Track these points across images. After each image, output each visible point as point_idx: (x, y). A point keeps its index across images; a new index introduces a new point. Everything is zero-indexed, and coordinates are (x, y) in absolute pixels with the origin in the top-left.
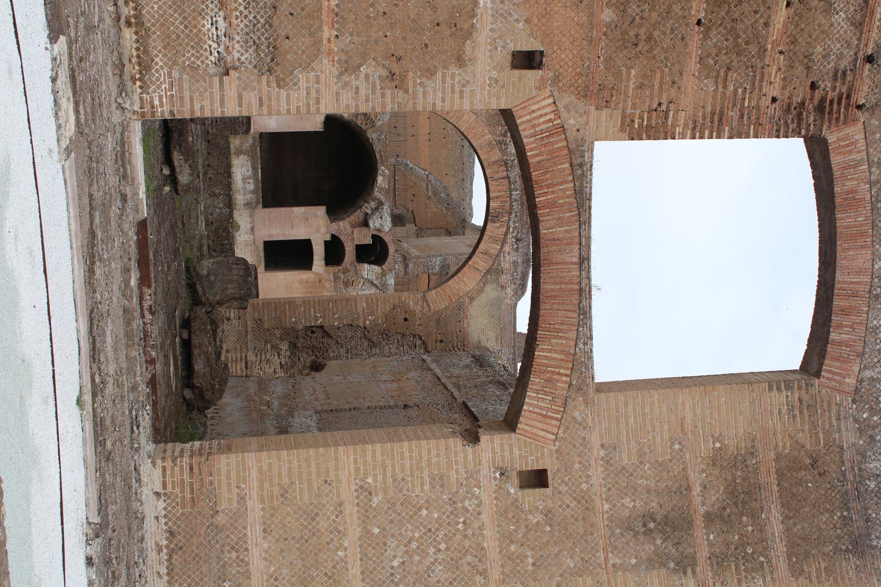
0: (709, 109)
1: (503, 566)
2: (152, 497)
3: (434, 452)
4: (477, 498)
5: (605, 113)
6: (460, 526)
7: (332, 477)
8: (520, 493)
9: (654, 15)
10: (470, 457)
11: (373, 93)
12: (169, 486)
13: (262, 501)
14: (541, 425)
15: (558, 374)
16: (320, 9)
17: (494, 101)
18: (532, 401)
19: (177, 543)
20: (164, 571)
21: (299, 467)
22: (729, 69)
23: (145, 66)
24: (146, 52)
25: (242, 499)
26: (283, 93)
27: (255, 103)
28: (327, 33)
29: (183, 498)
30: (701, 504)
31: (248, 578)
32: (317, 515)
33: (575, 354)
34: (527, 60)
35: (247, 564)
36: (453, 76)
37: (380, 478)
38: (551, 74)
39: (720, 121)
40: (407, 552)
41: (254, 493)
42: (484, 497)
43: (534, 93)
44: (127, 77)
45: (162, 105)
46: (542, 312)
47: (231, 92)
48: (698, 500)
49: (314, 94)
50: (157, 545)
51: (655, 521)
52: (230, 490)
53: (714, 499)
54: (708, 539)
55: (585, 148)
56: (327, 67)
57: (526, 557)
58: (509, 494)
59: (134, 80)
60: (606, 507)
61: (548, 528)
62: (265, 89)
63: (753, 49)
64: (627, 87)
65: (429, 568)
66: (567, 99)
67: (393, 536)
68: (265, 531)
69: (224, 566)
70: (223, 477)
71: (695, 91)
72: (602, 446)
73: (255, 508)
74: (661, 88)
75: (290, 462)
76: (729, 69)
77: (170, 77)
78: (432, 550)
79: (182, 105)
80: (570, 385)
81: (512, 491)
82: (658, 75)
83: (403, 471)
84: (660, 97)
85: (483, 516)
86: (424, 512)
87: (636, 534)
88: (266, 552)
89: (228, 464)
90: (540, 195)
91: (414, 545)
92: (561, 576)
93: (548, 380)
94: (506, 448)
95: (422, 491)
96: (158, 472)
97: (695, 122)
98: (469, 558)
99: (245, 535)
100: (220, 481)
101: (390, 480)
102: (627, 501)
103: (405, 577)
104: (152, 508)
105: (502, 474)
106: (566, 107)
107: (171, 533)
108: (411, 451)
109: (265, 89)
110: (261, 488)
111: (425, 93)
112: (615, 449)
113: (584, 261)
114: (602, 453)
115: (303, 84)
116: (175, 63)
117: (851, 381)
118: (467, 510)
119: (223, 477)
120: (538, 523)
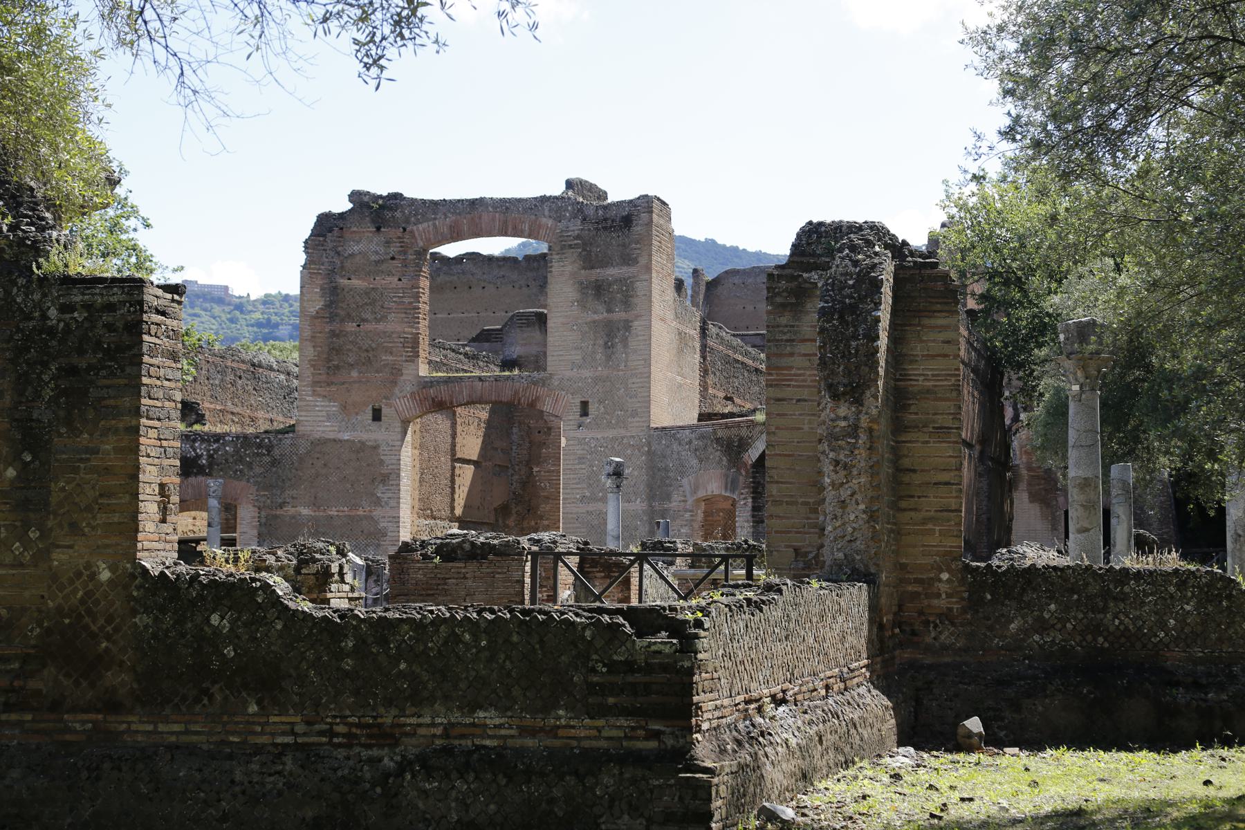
28: (360, 513)
34: (377, 416)
48: (601, 317)
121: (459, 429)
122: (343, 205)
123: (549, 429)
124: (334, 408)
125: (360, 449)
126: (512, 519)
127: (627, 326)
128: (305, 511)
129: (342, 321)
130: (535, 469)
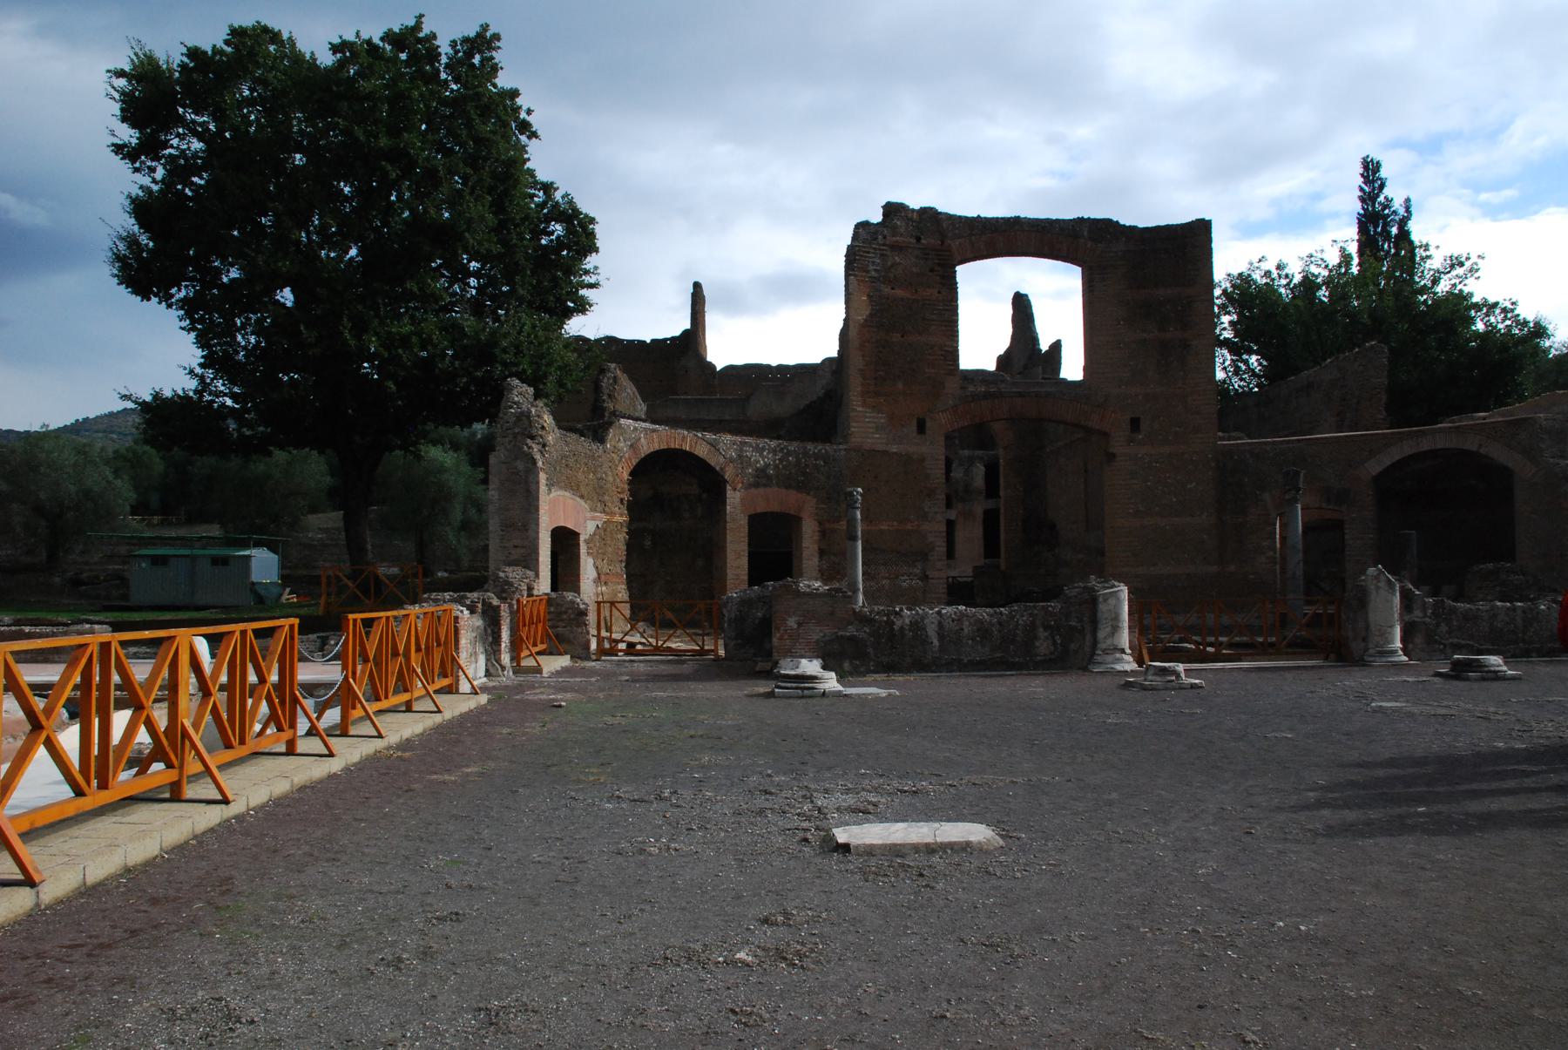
28: (909, 527)
34: (921, 428)
117: (1089, 244)
122: (876, 217)
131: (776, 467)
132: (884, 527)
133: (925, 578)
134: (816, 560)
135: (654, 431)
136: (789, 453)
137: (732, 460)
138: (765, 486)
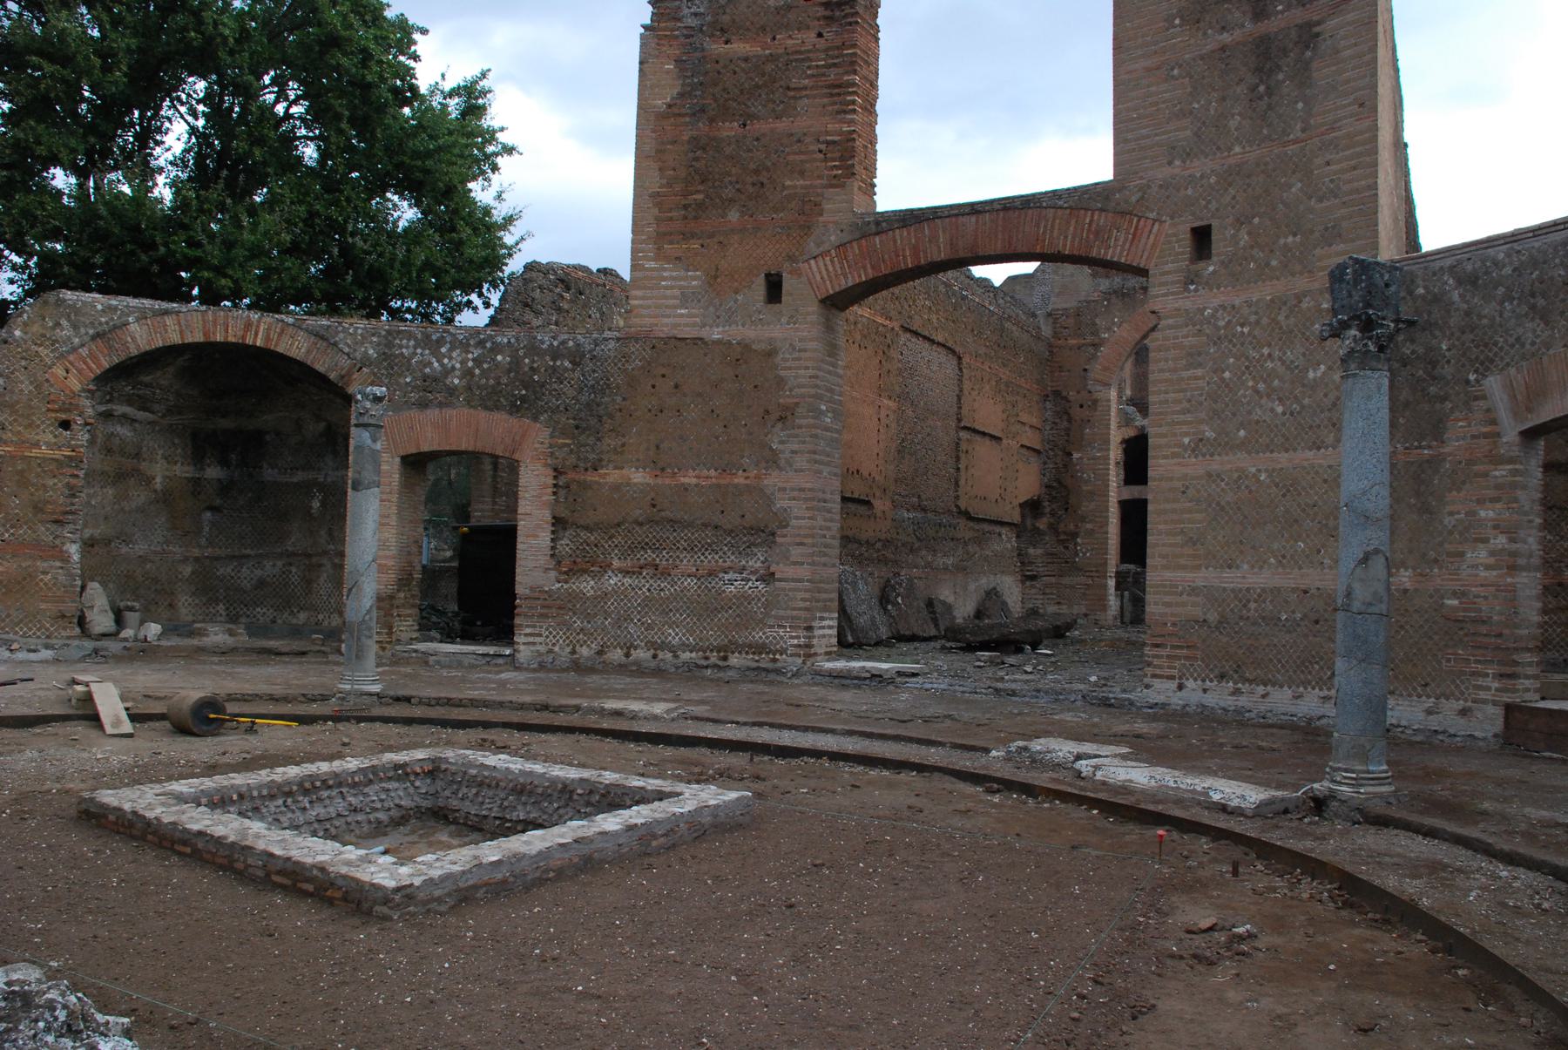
0: (826, 101)
1: (1293, 275)
2: (1183, 694)
3: (1162, 365)
4: (1216, 311)
5: (827, 206)
6: (1246, 330)
7: (1178, 484)
8: (1215, 259)
9: (734, 171)
10: (1170, 321)
11: (797, 436)
12: (1174, 672)
13: (1198, 567)
14: (1143, 241)
15: (1090, 224)
16: (719, 486)
17: (809, 318)
18: (1115, 252)
19: (1230, 670)
20: (1261, 689)
21: (1166, 522)
22: (788, 88)
23: (760, 649)
24: (750, 646)
25: (1194, 591)
26: (793, 522)
27: (800, 550)
28: (739, 480)
29: (1187, 658)
30: (1245, 28)
31: (1278, 589)
32: (1218, 504)
33: (1071, 208)
34: (774, 289)
35: (1263, 590)
36: (786, 360)
37: (1185, 429)
38: (787, 264)
39: (839, 86)
40: (1268, 396)
41: (1190, 575)
42: (1216, 302)
43: (804, 279)
44: (770, 666)
45: (798, 637)
46: (1025, 250)
47: (790, 571)
49: (795, 494)
50: (1233, 694)
51: (1257, 86)
52: (1184, 605)
53: (1237, 14)
54: (1282, 12)
55: (859, 222)
56: (772, 480)
57: (1285, 244)
58: (1214, 272)
59: (774, 660)
60: (1237, 149)
61: (1256, 220)
62: (788, 539)
63: (769, 67)
64: (802, 187)
65: (1288, 368)
66: (812, 248)
67: (1249, 413)
68: (1230, 567)
69: (1263, 618)
70: (1168, 610)
71: (811, 118)
72: (1170, 163)
73: (1206, 577)
74: (801, 153)
75: (1160, 533)
76: (788, 88)
77: (772, 627)
78: (1269, 364)
79: (799, 618)
80: (1102, 210)
81: (1211, 268)
82: (791, 158)
83: (1180, 402)
84: (813, 152)
85: (1237, 302)
86: (1227, 375)
87: (1270, 107)
88: (1253, 567)
89: (1156, 604)
90: (906, 263)
91: (1261, 386)
92: (1310, 198)
93: (1097, 233)
94: (1164, 279)
95: (1203, 378)
96: (1157, 683)
97: (838, 112)
98: (1281, 318)
99: (1233, 590)
100: (1172, 615)
101: (1189, 417)
102: (1233, 124)
103: (1296, 397)
104: (1193, 694)
105: (1192, 283)
106: (818, 246)
107: (1222, 677)
108: (1159, 393)
109: (788, 539)
110: (1184, 568)
111: (800, 386)
112: (1173, 148)
113: (974, 209)
114: (1177, 163)
115: (785, 504)
116: (761, 621)
118: (1229, 322)
119: (1168, 610)
120: (1249, 233)
121: (967, 385)
123: (1095, 402)
124: (695, 280)
125: (740, 356)
126: (1045, 520)
127: (1308, 36)
128: (638, 477)
129: (712, 120)
130: (1076, 456)
131: (468, 373)
132: (689, 479)
133: (768, 577)
134: (545, 538)
135: (166, 312)
136: (497, 348)
137: (366, 361)
138: (441, 405)
